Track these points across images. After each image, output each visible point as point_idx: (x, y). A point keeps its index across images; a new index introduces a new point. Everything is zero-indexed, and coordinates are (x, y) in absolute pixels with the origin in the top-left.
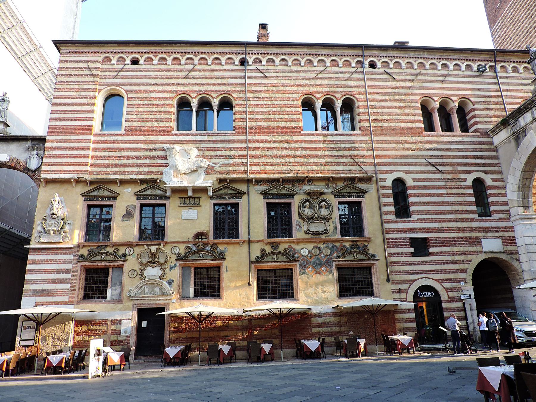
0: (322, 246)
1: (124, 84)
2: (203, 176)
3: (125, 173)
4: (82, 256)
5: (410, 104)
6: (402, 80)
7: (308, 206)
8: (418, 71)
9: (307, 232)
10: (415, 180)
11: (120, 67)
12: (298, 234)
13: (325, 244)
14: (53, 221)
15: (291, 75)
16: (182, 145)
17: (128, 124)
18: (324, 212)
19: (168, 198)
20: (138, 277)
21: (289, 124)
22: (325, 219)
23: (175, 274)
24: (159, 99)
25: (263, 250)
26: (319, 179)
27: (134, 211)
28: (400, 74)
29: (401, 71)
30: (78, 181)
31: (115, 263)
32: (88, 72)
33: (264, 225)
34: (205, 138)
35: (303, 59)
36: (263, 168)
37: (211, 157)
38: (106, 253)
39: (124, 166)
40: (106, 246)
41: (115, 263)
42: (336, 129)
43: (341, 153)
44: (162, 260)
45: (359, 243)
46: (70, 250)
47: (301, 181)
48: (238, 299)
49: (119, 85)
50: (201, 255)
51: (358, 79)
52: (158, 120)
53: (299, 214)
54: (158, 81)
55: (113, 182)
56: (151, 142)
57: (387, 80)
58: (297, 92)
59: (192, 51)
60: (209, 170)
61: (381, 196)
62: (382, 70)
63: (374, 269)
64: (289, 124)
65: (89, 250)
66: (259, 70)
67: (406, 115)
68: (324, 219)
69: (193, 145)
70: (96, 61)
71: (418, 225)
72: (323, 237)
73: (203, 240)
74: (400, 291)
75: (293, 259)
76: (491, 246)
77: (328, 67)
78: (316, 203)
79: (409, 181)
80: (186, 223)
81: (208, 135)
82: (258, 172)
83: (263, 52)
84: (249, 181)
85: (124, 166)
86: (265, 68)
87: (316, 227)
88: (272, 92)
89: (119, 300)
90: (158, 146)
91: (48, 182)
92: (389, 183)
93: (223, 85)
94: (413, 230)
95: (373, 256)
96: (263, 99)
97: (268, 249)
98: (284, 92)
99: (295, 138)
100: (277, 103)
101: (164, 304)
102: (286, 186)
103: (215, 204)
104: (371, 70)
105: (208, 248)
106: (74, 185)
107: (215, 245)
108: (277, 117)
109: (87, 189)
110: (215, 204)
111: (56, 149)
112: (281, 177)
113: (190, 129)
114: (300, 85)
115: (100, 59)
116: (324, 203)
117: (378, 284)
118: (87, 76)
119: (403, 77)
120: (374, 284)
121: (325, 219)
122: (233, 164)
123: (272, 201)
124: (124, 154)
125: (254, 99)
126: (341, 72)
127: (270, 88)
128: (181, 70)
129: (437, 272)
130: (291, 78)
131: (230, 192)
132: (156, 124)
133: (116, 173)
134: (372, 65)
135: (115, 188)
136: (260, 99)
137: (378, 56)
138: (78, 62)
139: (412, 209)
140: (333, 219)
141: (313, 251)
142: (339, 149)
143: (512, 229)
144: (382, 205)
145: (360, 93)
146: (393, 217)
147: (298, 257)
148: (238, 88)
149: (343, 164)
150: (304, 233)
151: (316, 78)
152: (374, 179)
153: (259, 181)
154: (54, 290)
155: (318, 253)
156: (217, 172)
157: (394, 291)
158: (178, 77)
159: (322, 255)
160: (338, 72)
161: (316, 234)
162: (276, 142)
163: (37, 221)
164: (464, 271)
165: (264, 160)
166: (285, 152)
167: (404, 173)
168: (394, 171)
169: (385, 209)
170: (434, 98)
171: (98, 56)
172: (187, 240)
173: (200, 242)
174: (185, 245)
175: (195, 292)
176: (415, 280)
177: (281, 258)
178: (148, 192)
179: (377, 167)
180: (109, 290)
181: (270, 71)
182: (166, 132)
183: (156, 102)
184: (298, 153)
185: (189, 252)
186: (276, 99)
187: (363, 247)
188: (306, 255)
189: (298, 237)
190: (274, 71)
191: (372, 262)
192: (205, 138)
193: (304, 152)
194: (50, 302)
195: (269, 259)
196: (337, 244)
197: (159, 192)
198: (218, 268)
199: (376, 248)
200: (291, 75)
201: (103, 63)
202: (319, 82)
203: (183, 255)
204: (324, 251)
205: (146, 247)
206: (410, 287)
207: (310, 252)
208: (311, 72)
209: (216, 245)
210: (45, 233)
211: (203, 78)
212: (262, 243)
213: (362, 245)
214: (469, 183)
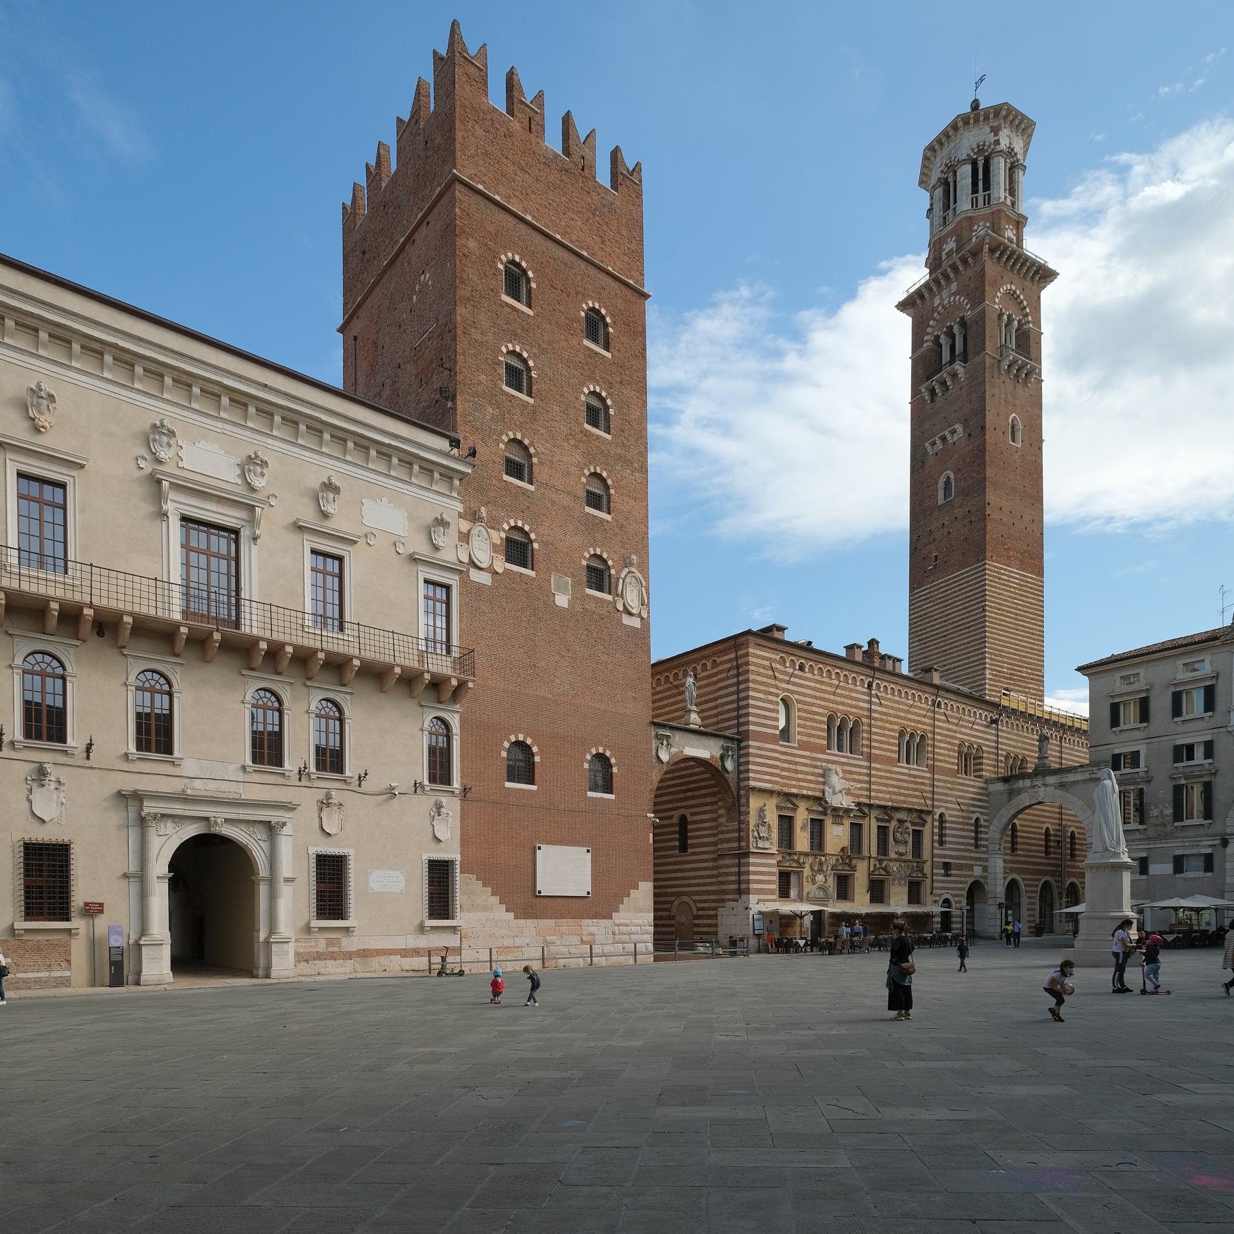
3: (800, 787)
26: (905, 809)
30: (779, 793)
47: (897, 809)
48: (861, 904)
55: (796, 796)
58: (895, 723)
60: (848, 792)
63: (923, 884)
67: (949, 756)
71: (947, 853)
75: (888, 874)
76: (978, 871)
84: (870, 806)
87: (902, 849)
92: (937, 817)
122: (861, 789)
124: (799, 768)
129: (953, 889)
133: (794, 787)
134: (939, 706)
143: (986, 860)
156: (853, 795)
162: (886, 771)
164: (963, 889)
181: (887, 700)
199: (927, 869)
202: (910, 716)
214: (973, 822)
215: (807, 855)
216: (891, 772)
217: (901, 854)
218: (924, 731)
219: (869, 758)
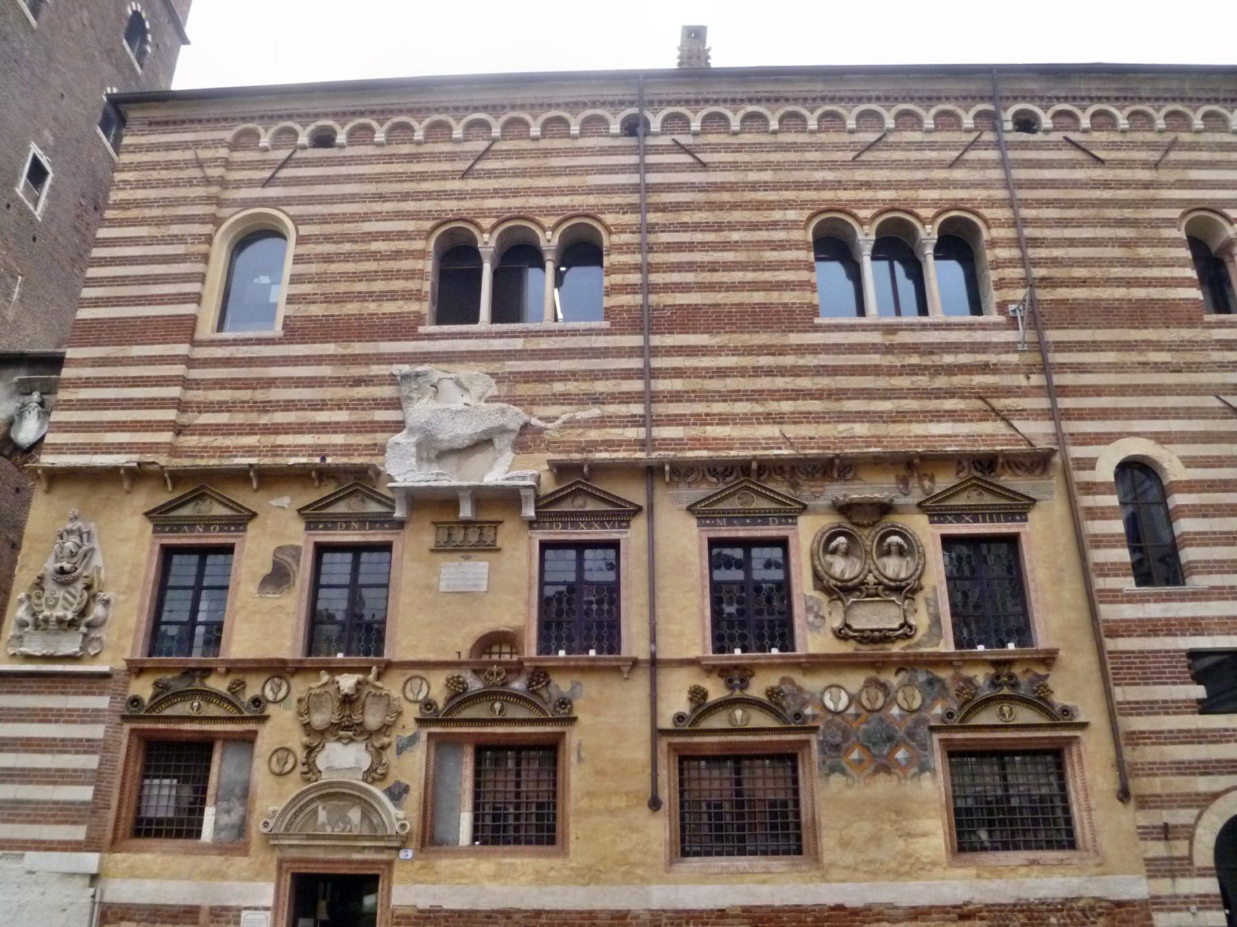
0: (893, 679)
1: (289, 201)
2: (509, 455)
3: (275, 450)
4: (136, 701)
5: (1150, 233)
6: (1122, 164)
7: (842, 547)
8: (1169, 137)
9: (841, 634)
10: (1189, 462)
11: (282, 154)
12: (813, 639)
13: (902, 675)
14: (61, 593)
15: (776, 157)
16: (445, 366)
17: (292, 310)
18: (894, 567)
19: (401, 524)
20: (296, 775)
21: (774, 297)
22: (904, 590)
23: (412, 766)
24: (386, 236)
25: (697, 695)
26: (878, 462)
27: (295, 567)
28: (1114, 146)
29: (1116, 137)
30: (138, 475)
31: (230, 727)
32: (195, 173)
33: (702, 610)
34: (518, 344)
35: (812, 111)
36: (695, 431)
37: (533, 401)
38: (209, 696)
39: (276, 429)
40: (207, 672)
41: (230, 727)
42: (923, 309)
43: (942, 382)
44: (373, 719)
45: (1017, 670)
46: (102, 683)
49: (277, 202)
50: (497, 706)
51: (984, 165)
52: (381, 297)
53: (817, 576)
54: (386, 188)
55: (240, 476)
56: (355, 359)
57: (1073, 164)
58: (801, 205)
59: (485, 103)
61: (1081, 514)
62: (1057, 136)
64: (774, 297)
65: (156, 684)
66: (682, 147)
68: (898, 590)
69: (483, 367)
70: (217, 143)
72: (896, 648)
73: (506, 657)
74: (1166, 832)
77: (890, 131)
78: (868, 537)
79: (1172, 464)
80: (451, 603)
81: (527, 334)
82: (679, 443)
83: (692, 96)
84: (650, 473)
85: (276, 429)
86: (701, 140)
87: (871, 617)
88: (721, 206)
89: (236, 840)
90: (376, 370)
91: (56, 477)
93: (573, 191)
94: (1196, 626)
95: (1066, 711)
96: (696, 227)
97: (716, 690)
98: (759, 206)
99: (795, 338)
100: (735, 236)
101: (374, 862)
102: (770, 486)
103: (545, 546)
104: (1024, 136)
105: (518, 685)
106: (126, 486)
107: (540, 675)
108: (737, 276)
109: (163, 498)
110: (545, 546)
111: (88, 383)
112: (754, 458)
113: (475, 320)
114: (808, 186)
115: (228, 135)
116: (895, 539)
117: (1089, 809)
118: (190, 183)
119: (1121, 155)
120: (1075, 809)
121: (904, 590)
122: (601, 422)
123: (725, 532)
125: (666, 228)
126: (932, 146)
127: (714, 197)
128: (451, 157)
130: (778, 167)
131: (591, 506)
132: (372, 307)
134: (1026, 123)
135: (247, 498)
136: (685, 227)
137: (1041, 98)
138: (169, 147)
139: (1188, 554)
140: (927, 589)
141: (864, 696)
142: (937, 370)
144: (1087, 542)
145: (992, 203)
146: (1128, 584)
147: (815, 717)
148: (617, 199)
149: (954, 416)
150: (831, 635)
151: (855, 163)
152: (1057, 459)
153: (682, 472)
154: (46, 802)
155: (879, 704)
156: (551, 445)
157: (1146, 833)
158: (443, 176)
159: (895, 711)
160: (920, 146)
161: (873, 641)
162: (736, 351)
163: (19, 592)
165: (700, 408)
166: (764, 383)
167: (1152, 443)
168: (1121, 435)
169: (1099, 556)
170: (1226, 211)
171: (224, 128)
172: (455, 658)
173: (492, 663)
174: (448, 673)
175: (476, 828)
176: (1216, 796)
177: (760, 719)
178: (341, 508)
179: (1063, 424)
180: (209, 814)
182: (403, 328)
183: (376, 246)
184: (805, 383)
185: (459, 697)
186: (732, 227)
187: (1032, 683)
188: (841, 707)
189: (812, 650)
190: (727, 148)
191: (1065, 733)
192: (518, 344)
193: (824, 382)
194: (34, 842)
195: (717, 721)
196: (945, 674)
197: (373, 508)
198: (550, 749)
199: (1076, 686)
200: (776, 157)
201: (234, 146)
202: (861, 175)
203: (441, 705)
204: (900, 696)
205: (325, 678)
206: (1199, 817)
207: (853, 699)
208: (838, 147)
209: (546, 675)
210: (37, 627)
211: (515, 175)
212: (694, 670)
213: (1029, 675)
215: (278, 669)
216: (781, 351)
217: (866, 637)
218: (956, 205)
219: (645, 321)
